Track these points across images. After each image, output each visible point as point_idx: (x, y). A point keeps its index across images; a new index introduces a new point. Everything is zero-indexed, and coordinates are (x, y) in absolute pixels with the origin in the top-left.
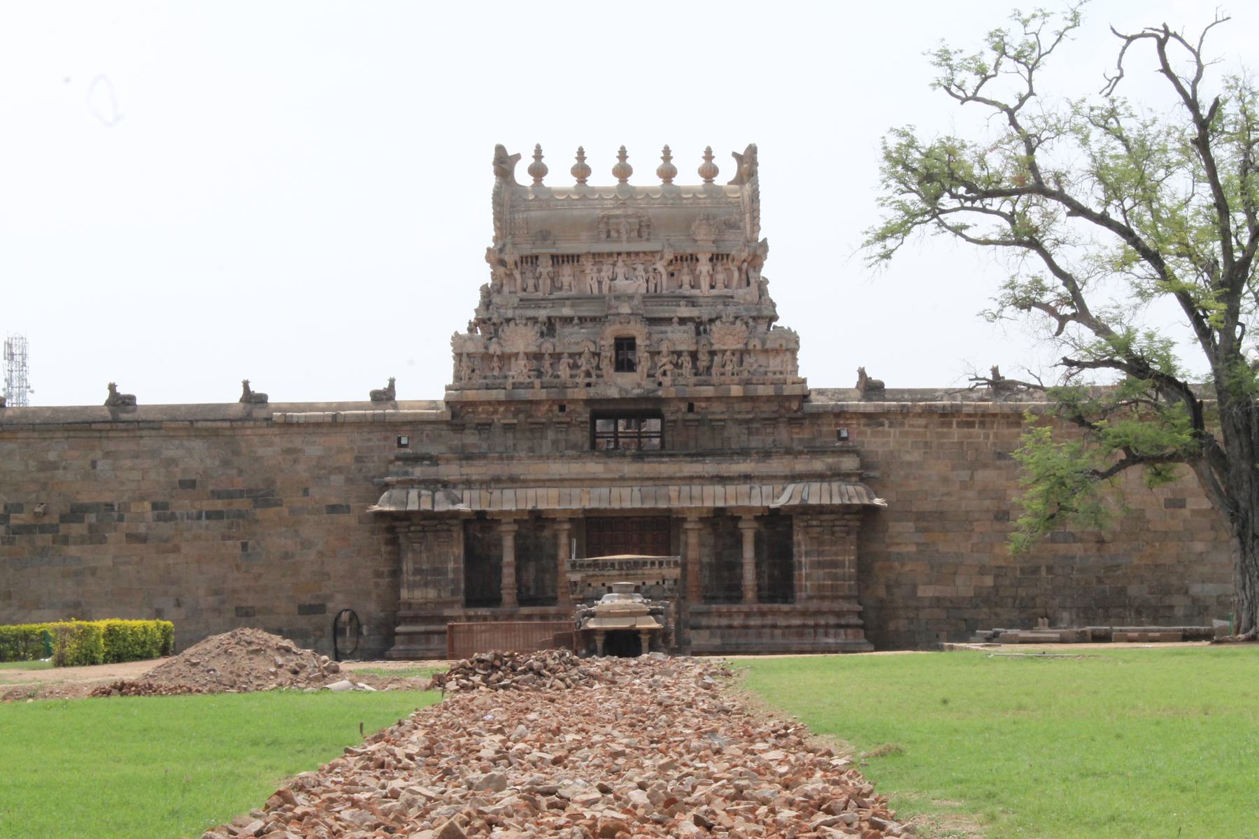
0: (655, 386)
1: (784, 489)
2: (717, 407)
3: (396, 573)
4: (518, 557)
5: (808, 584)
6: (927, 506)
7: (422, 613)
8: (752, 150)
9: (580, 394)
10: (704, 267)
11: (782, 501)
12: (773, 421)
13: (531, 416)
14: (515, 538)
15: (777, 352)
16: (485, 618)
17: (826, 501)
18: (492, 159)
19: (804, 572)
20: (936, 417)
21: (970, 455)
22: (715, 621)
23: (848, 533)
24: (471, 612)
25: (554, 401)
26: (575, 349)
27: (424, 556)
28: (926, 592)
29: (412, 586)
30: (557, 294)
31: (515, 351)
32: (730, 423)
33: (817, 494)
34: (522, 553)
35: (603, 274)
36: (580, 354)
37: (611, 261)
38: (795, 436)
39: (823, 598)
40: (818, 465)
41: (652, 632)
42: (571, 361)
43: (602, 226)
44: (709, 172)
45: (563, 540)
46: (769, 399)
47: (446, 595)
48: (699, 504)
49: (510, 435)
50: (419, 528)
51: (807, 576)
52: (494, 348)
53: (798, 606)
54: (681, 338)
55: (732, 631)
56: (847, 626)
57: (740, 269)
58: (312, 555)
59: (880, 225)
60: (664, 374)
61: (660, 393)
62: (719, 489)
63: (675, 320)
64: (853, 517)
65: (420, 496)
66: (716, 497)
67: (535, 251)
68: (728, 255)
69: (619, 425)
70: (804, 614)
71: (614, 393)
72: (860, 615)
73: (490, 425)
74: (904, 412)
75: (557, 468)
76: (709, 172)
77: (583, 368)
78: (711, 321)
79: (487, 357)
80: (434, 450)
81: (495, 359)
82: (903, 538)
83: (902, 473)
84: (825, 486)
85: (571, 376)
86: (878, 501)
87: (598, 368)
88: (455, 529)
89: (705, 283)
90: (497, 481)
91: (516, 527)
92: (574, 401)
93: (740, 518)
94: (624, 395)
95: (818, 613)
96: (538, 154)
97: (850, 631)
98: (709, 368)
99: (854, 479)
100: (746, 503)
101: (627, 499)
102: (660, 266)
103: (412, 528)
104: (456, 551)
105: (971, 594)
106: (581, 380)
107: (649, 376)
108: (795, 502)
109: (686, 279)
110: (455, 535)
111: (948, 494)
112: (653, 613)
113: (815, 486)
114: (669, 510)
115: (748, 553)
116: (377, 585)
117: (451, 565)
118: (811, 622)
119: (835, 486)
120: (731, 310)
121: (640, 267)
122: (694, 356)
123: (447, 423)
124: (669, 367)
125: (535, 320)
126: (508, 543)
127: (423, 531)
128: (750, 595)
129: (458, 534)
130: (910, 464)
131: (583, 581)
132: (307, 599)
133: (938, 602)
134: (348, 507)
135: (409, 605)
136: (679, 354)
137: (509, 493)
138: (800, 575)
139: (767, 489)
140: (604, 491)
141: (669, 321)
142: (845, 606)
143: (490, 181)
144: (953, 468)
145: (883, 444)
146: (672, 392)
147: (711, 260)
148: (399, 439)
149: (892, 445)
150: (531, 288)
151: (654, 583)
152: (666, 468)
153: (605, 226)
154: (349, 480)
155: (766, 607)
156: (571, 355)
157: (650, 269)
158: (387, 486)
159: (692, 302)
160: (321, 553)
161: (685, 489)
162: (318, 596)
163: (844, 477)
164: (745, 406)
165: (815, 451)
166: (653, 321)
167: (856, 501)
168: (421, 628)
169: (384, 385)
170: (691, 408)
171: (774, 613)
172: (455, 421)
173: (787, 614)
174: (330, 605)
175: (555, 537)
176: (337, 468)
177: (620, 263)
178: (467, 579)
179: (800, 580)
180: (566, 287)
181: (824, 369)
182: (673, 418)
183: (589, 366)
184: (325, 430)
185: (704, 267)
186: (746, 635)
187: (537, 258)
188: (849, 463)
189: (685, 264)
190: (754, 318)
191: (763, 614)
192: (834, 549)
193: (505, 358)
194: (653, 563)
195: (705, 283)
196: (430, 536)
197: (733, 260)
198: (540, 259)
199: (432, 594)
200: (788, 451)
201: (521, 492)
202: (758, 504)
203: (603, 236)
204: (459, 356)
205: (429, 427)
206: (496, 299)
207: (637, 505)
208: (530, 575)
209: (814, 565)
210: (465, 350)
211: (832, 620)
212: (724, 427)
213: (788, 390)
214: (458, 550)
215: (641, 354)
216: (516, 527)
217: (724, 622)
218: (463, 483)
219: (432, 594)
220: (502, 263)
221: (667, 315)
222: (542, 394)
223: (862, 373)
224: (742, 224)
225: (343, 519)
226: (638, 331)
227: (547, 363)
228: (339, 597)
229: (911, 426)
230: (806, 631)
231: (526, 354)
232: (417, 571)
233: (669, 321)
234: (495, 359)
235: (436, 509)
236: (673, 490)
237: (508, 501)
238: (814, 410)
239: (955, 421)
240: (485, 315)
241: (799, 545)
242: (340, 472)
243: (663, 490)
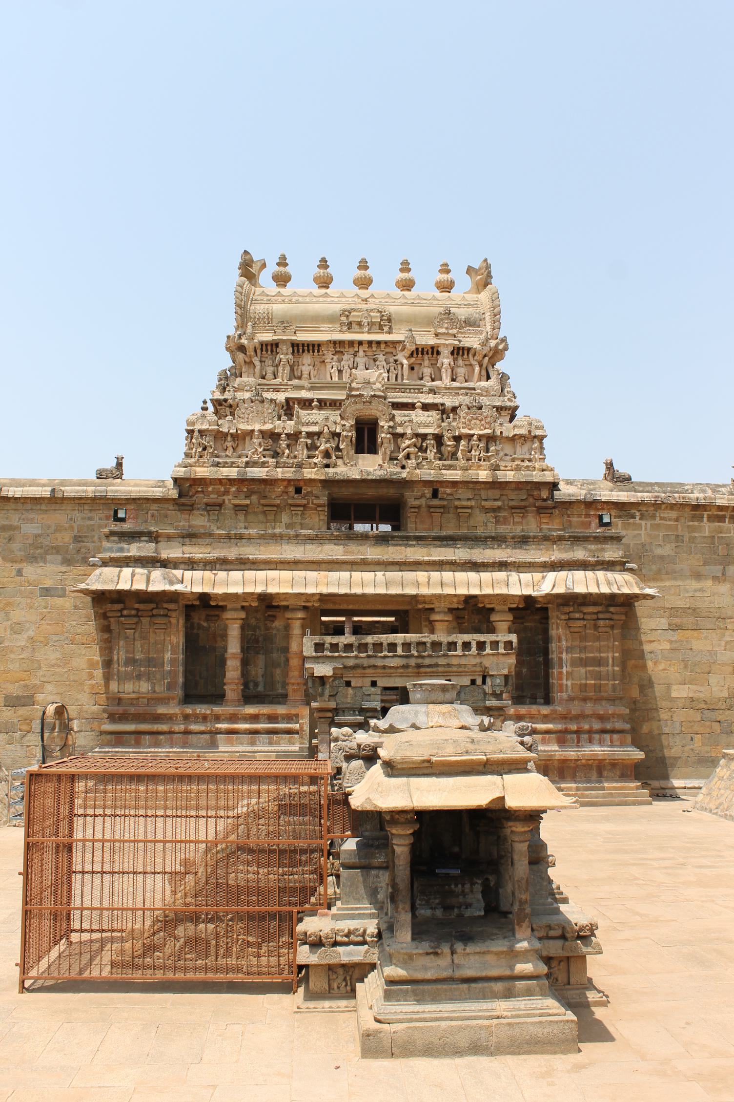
0: (399, 470)
1: (544, 578)
2: (462, 493)
5: (569, 683)
7: (132, 710)
10: (445, 360)
12: (521, 509)
13: (265, 497)
14: (243, 628)
16: (205, 718)
17: (593, 589)
18: (238, 265)
19: (564, 670)
20: (687, 509)
21: (721, 550)
23: (612, 627)
24: (189, 710)
25: (289, 481)
26: (315, 429)
27: (138, 644)
28: (680, 692)
29: (129, 677)
30: (295, 382)
31: (250, 428)
32: (477, 511)
33: (583, 583)
34: (251, 646)
35: (342, 363)
36: (319, 434)
37: (352, 351)
38: (544, 526)
39: (585, 700)
40: (579, 554)
42: (309, 441)
43: (343, 319)
45: (296, 630)
48: (451, 591)
49: (241, 517)
50: (133, 612)
51: (567, 675)
54: (426, 422)
56: (612, 731)
57: (481, 366)
58: (22, 641)
60: (408, 457)
61: (404, 475)
62: (472, 576)
63: (418, 404)
64: (618, 609)
65: (133, 575)
67: (276, 338)
68: (469, 349)
70: (564, 718)
73: (220, 505)
77: (322, 448)
79: (220, 436)
81: (229, 438)
83: (654, 567)
84: (589, 574)
85: (309, 457)
87: (338, 449)
88: (174, 614)
90: (223, 564)
91: (243, 615)
93: (492, 610)
94: (365, 477)
95: (580, 717)
96: (283, 262)
97: (615, 736)
98: (454, 456)
99: (618, 568)
100: (504, 591)
103: (125, 612)
104: (174, 639)
105: (725, 694)
107: (391, 459)
108: (560, 590)
109: (427, 371)
110: (173, 621)
111: (701, 590)
113: (579, 574)
114: (415, 597)
116: (91, 677)
117: (168, 656)
118: (574, 727)
119: (600, 574)
121: (381, 357)
122: (439, 439)
123: (174, 499)
124: (412, 450)
126: (234, 632)
127: (137, 616)
129: (178, 621)
130: (661, 557)
131: (335, 677)
132: (15, 690)
134: (64, 590)
136: (424, 437)
137: (236, 575)
138: (561, 673)
139: (526, 577)
141: (411, 406)
143: (234, 276)
144: (705, 563)
145: (635, 536)
147: (452, 353)
149: (644, 539)
150: (270, 375)
151: (466, 681)
156: (310, 435)
157: (392, 360)
161: (435, 575)
162: (26, 686)
164: (492, 493)
165: (577, 540)
166: (397, 406)
167: (626, 590)
168: (131, 727)
169: (114, 463)
170: (435, 494)
172: (183, 500)
173: (546, 719)
174: (39, 697)
175: (287, 627)
176: (52, 547)
177: (361, 353)
178: (187, 673)
179: (561, 679)
180: (305, 376)
182: (417, 503)
183: (328, 445)
184: (44, 507)
185: (445, 360)
187: (277, 345)
189: (426, 357)
190: (499, 409)
192: (597, 644)
193: (240, 438)
194: (466, 645)
196: (145, 621)
197: (474, 355)
198: (280, 346)
201: (249, 574)
202: (519, 593)
203: (345, 328)
205: (155, 506)
207: (382, 591)
209: (574, 663)
210: (197, 427)
211: (597, 726)
212: (470, 515)
213: (537, 477)
214: (177, 639)
215: (382, 435)
216: (243, 615)
218: (184, 563)
219: (144, 687)
221: (410, 401)
222: (280, 473)
223: (610, 466)
224: (481, 323)
227: (283, 444)
228: (49, 687)
229: (661, 518)
230: (569, 736)
231: (261, 431)
233: (411, 406)
234: (229, 438)
235: (151, 589)
236: (422, 576)
238: (563, 498)
239: (705, 514)
240: (218, 396)
241: (560, 640)
242: (58, 553)
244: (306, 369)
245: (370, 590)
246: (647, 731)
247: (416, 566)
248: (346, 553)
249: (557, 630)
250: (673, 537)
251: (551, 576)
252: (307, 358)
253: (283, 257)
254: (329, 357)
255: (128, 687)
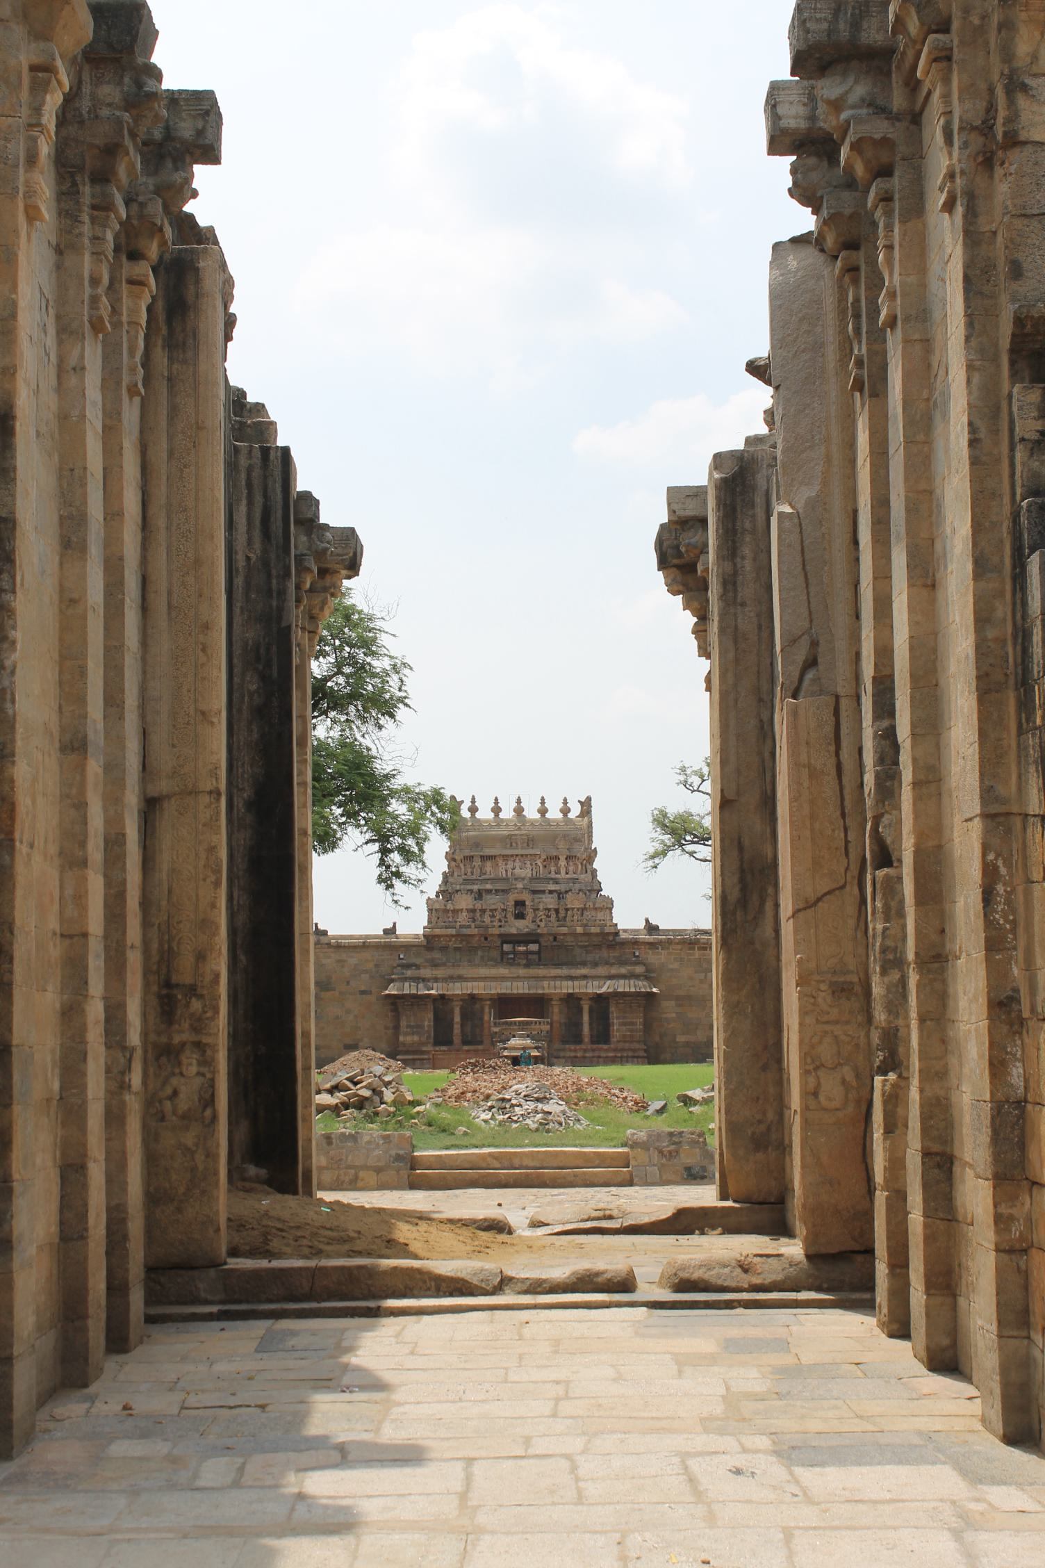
2: (569, 939)
3: (397, 1027)
4: (462, 1019)
6: (681, 993)
8: (589, 799)
9: (496, 931)
10: (562, 863)
11: (604, 990)
12: (599, 947)
15: (601, 909)
17: (627, 990)
22: (568, 1054)
26: (493, 907)
28: (681, 1039)
29: (406, 1034)
33: (622, 986)
34: (465, 1016)
40: (623, 970)
41: (536, 1057)
44: (565, 811)
45: (487, 1010)
46: (597, 934)
47: (423, 1039)
51: (617, 1030)
52: (449, 906)
54: (550, 901)
59: (652, 851)
62: (570, 983)
66: (568, 987)
70: (615, 1050)
71: (514, 931)
72: (645, 1051)
74: (670, 942)
75: (483, 971)
76: (565, 811)
78: (567, 892)
79: (446, 911)
80: (418, 961)
82: (669, 1009)
86: (654, 990)
89: (563, 872)
90: (452, 978)
92: (492, 935)
95: (623, 1050)
96: (473, 801)
101: (521, 988)
102: (539, 862)
106: (496, 924)
108: (611, 990)
109: (553, 869)
112: (536, 1048)
113: (622, 982)
115: (586, 1018)
120: (577, 886)
125: (471, 891)
126: (457, 1011)
128: (586, 1040)
129: (430, 1007)
130: (672, 970)
132: (348, 1041)
133: (687, 1044)
135: (404, 1044)
136: (549, 910)
137: (458, 985)
140: (509, 984)
141: (543, 892)
142: (637, 1046)
146: (545, 931)
152: (541, 971)
153: (509, 840)
154: (372, 977)
155: (595, 1046)
158: (392, 981)
159: (556, 881)
160: (356, 1016)
163: (637, 977)
165: (622, 963)
166: (534, 892)
170: (555, 939)
171: (600, 1050)
181: (627, 919)
185: (562, 863)
188: (639, 969)
191: (593, 1050)
193: (455, 912)
195: (563, 872)
199: (416, 1038)
200: (607, 963)
201: (464, 984)
204: (430, 910)
206: (451, 880)
208: (468, 1029)
211: (630, 1054)
213: (607, 930)
214: (431, 1015)
217: (573, 1054)
219: (416, 1038)
220: (454, 860)
223: (647, 921)
225: (368, 997)
226: (526, 897)
227: (478, 914)
228: (366, 1040)
232: (408, 1026)
233: (543, 892)
236: (546, 983)
237: (457, 989)
243: (540, 984)
244: (488, 869)
245: (521, 991)
247: (544, 978)
249: (614, 1010)
251: (608, 982)
252: (489, 864)
253: (473, 798)
254: (501, 862)
255: (409, 1039)
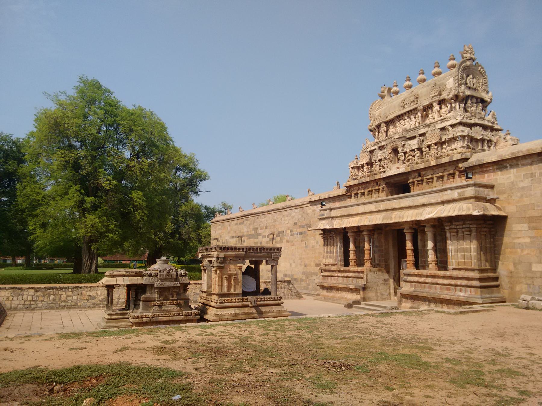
39: (460, 269)
53: (447, 273)
55: (419, 284)
69: (399, 185)
70: (451, 278)
95: (457, 278)
97: (472, 289)
118: (453, 282)
122: (420, 149)
130: (523, 188)
136: (413, 150)
142: (471, 274)
145: (508, 178)
148: (322, 203)
186: (425, 287)
211: (464, 282)
222: (368, 179)
246: (519, 290)
248: (376, 208)
250: (529, 175)
